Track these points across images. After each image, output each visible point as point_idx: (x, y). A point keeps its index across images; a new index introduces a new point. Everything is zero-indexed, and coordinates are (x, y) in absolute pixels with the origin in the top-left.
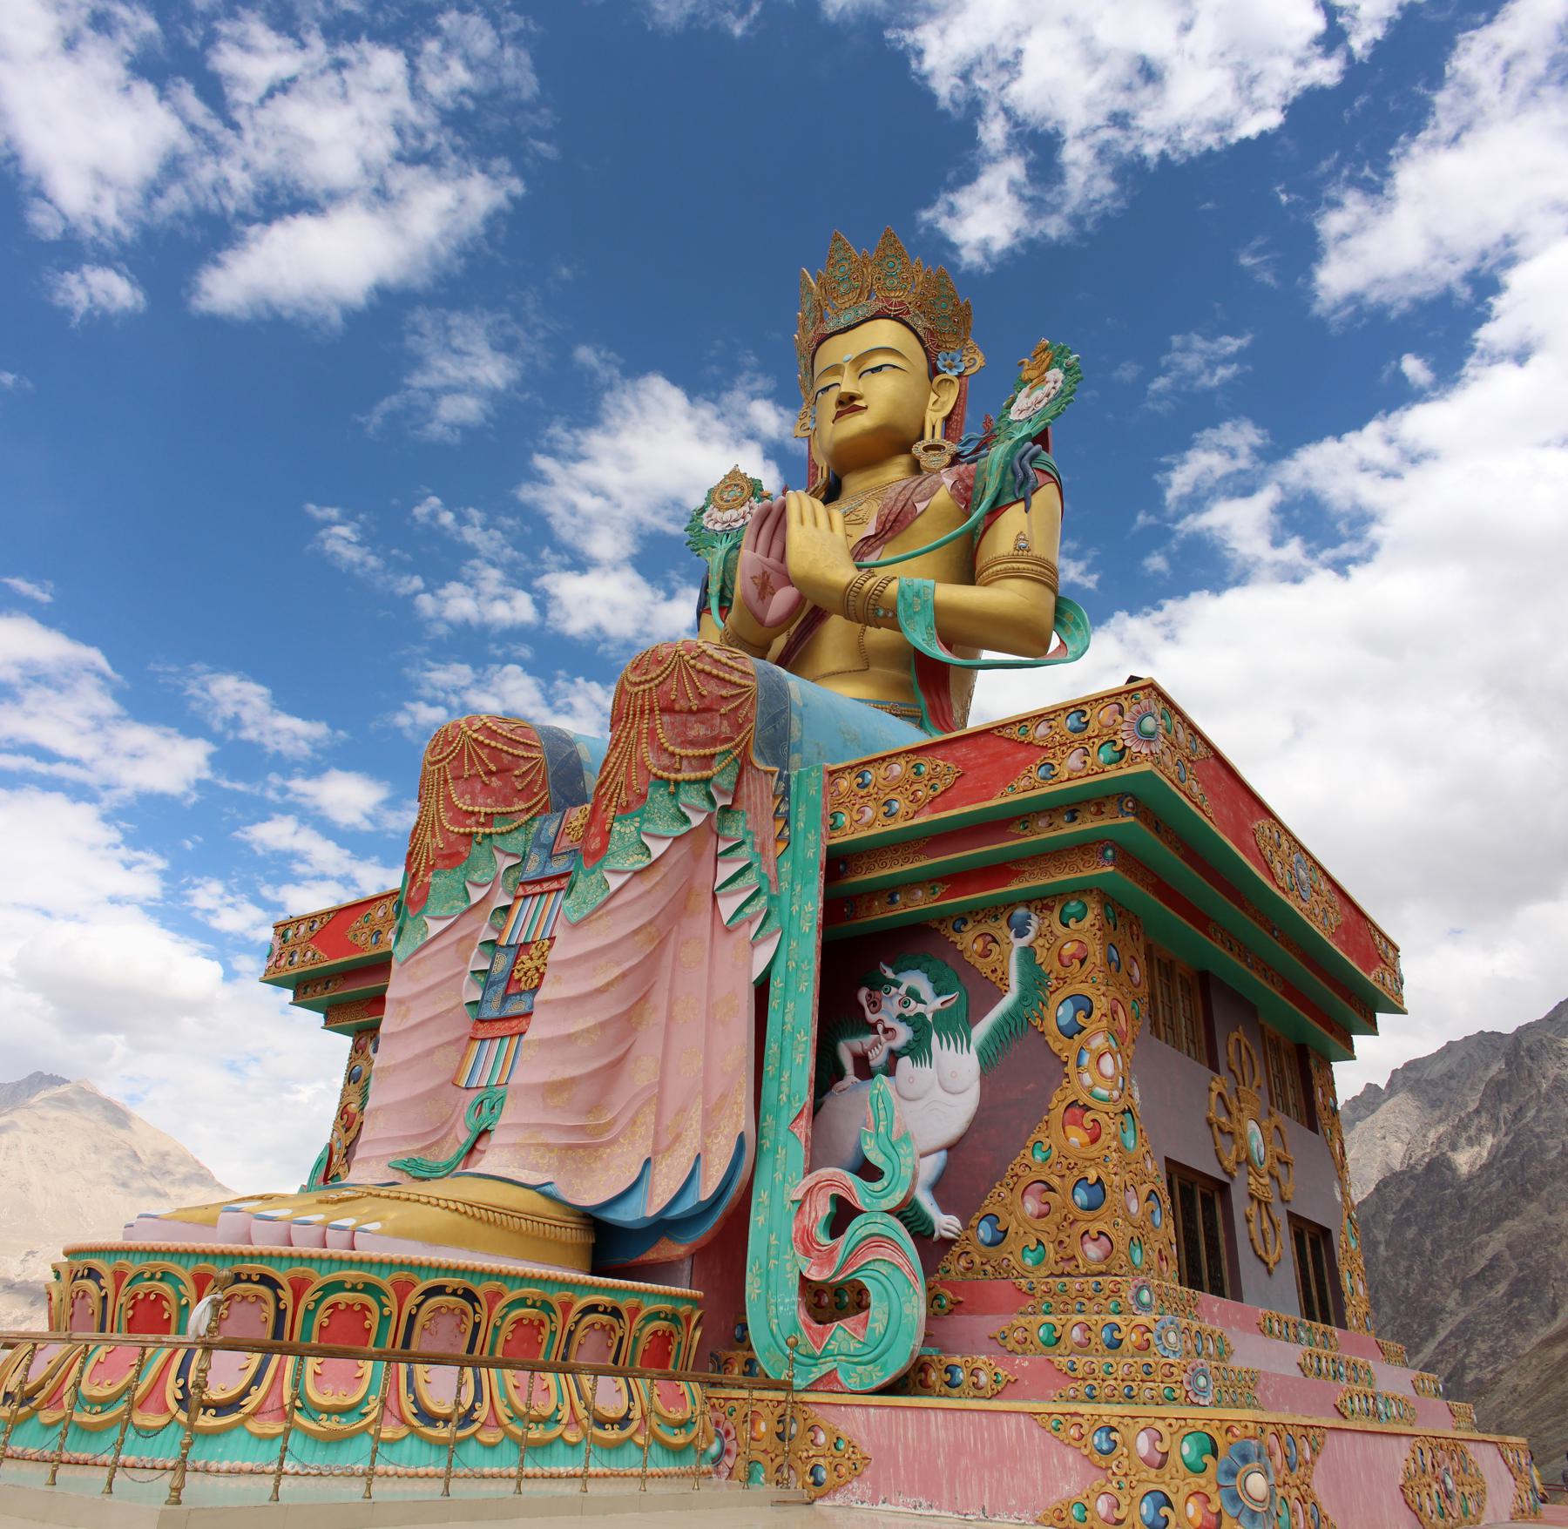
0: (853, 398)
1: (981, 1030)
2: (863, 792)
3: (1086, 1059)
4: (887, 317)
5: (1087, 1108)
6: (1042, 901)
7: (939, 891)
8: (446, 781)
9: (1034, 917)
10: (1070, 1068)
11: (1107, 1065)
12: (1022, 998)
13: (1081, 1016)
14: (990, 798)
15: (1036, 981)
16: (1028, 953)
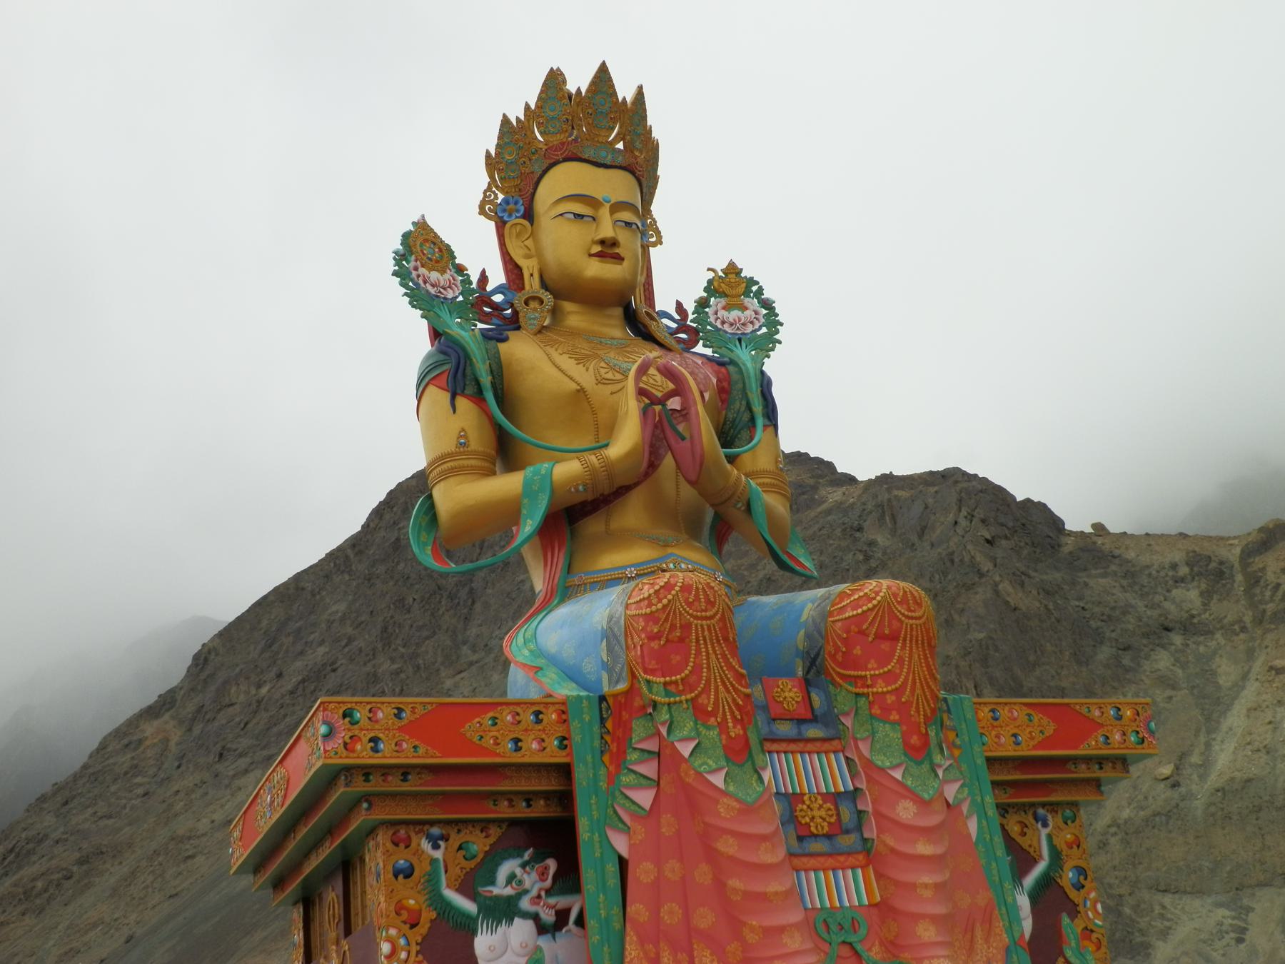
0: (614, 243)
1: (1030, 880)
2: (995, 723)
3: (1088, 903)
4: (633, 173)
5: (1092, 931)
6: (1053, 807)
7: (1010, 791)
8: (718, 641)
9: (1049, 817)
10: (1081, 908)
11: (1099, 907)
12: (1050, 867)
13: (1082, 878)
14: (1076, 748)
15: (1057, 857)
16: (1049, 837)
